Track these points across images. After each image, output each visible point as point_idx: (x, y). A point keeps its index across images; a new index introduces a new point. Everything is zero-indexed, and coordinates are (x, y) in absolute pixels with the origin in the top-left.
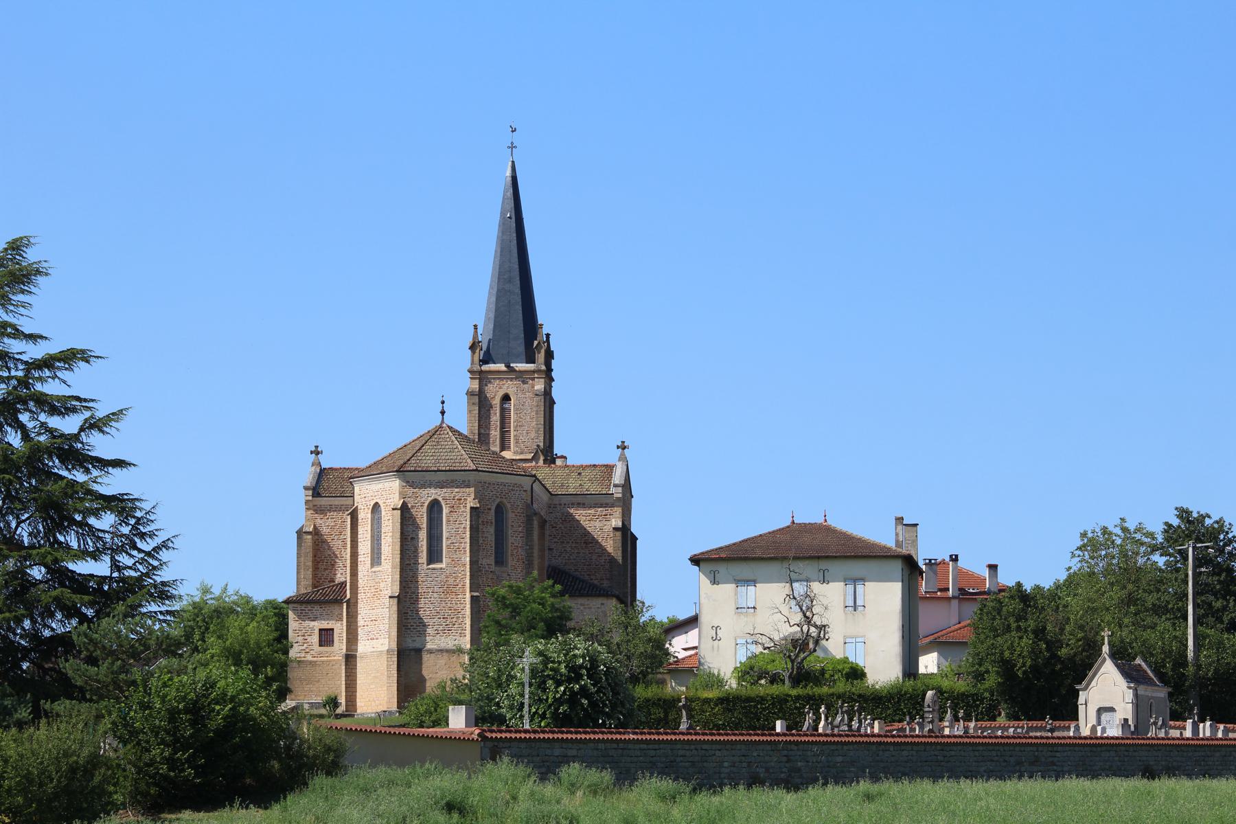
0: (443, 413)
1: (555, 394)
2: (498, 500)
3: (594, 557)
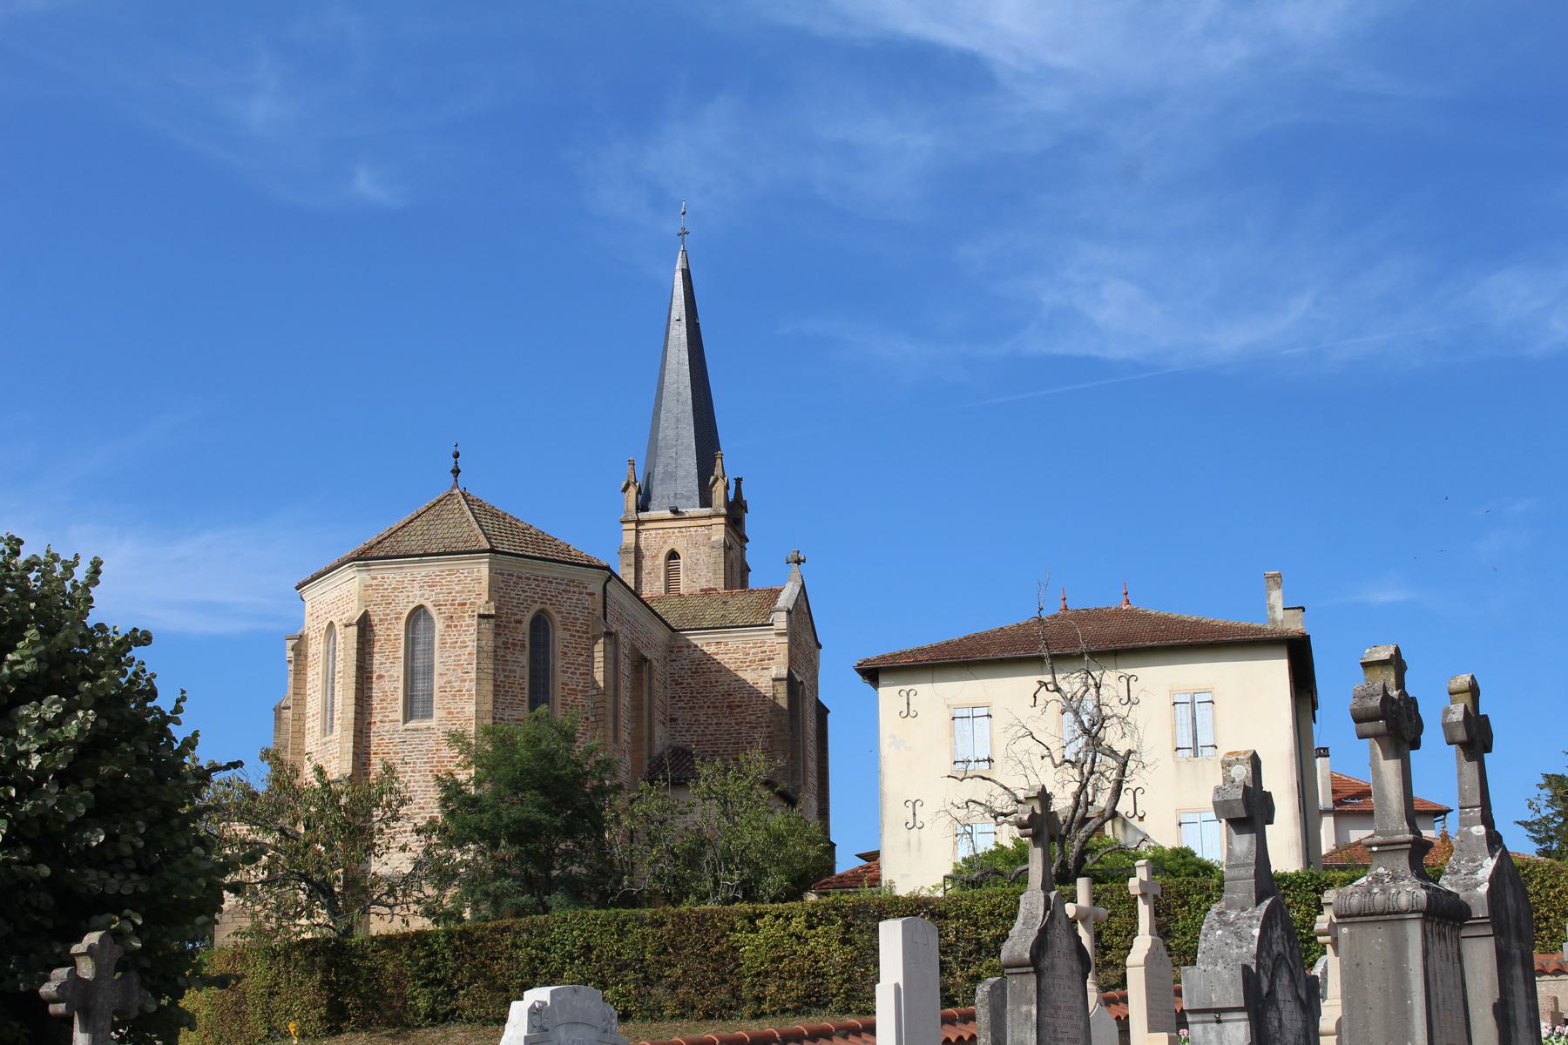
0: (456, 472)
1: (750, 559)
2: (537, 607)
3: (744, 730)
